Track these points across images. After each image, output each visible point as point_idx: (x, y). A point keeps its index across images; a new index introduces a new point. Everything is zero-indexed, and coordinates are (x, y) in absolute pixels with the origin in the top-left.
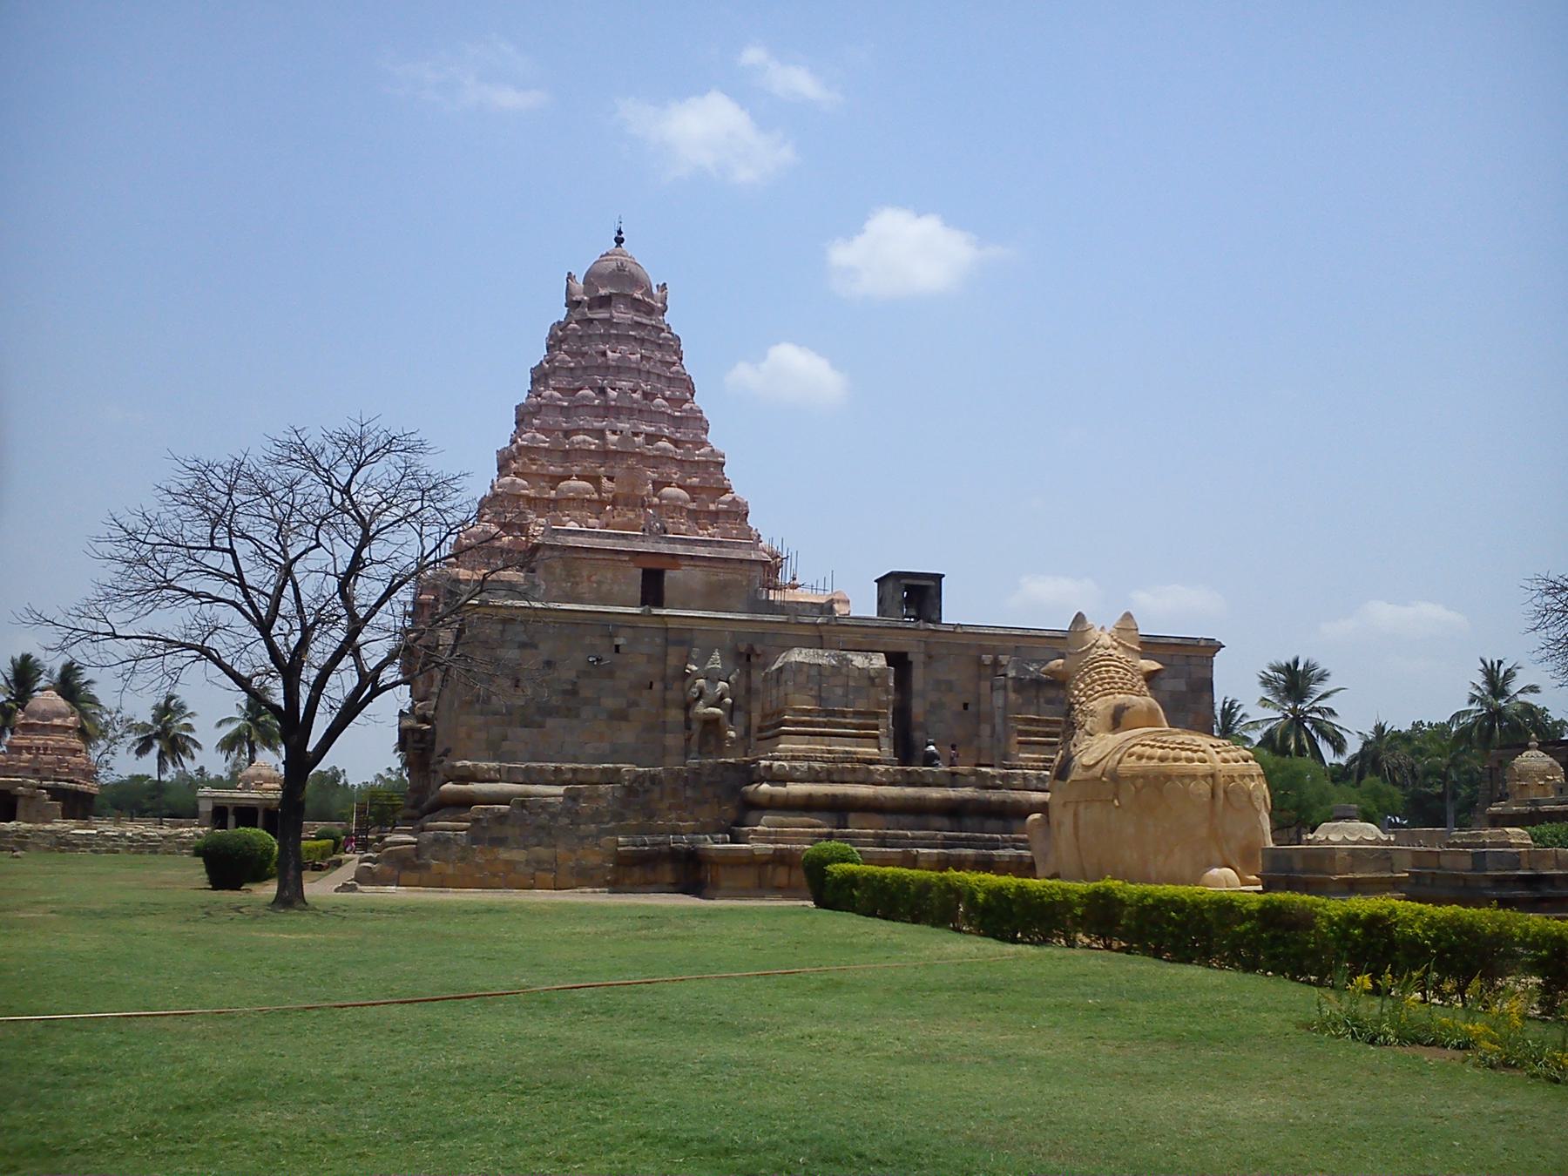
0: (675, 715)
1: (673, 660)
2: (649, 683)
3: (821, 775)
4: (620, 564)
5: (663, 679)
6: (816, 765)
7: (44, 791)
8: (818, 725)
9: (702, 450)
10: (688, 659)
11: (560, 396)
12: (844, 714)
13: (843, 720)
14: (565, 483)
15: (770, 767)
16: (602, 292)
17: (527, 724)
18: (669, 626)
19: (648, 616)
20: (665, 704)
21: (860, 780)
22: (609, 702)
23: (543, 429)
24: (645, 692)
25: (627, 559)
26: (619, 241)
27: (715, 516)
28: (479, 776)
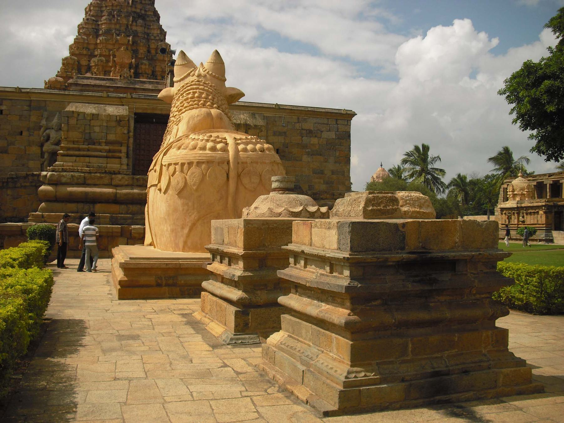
0: (35, 150)
1: (33, 118)
2: (20, 131)
3: (79, 180)
5: (28, 129)
6: (76, 174)
8: (83, 150)
12: (100, 144)
13: (98, 147)
15: (46, 175)
18: (32, 99)
19: (19, 93)
24: (18, 137)
25: (112, 90)
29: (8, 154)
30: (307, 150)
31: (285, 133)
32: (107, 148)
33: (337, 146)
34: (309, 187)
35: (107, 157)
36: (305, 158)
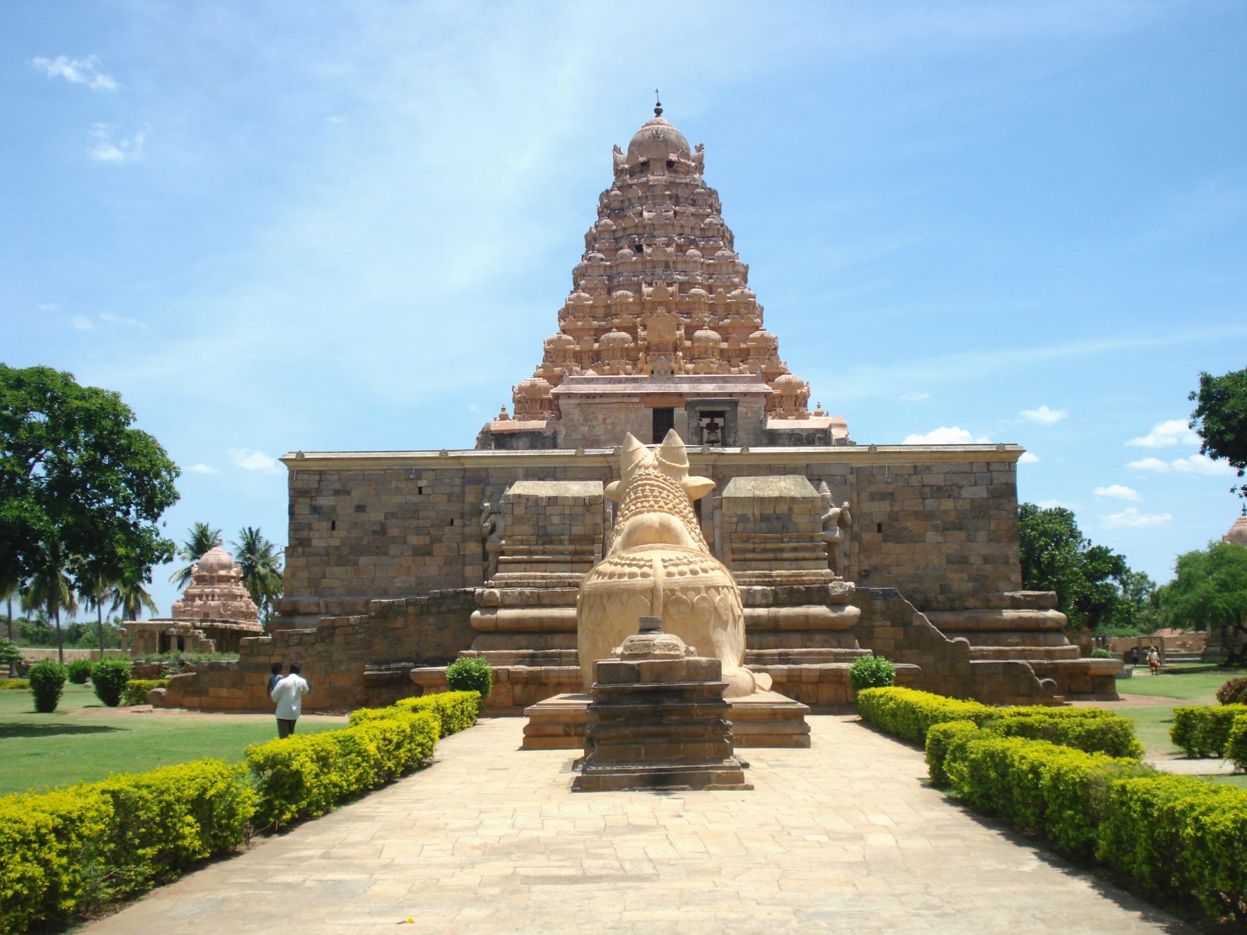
0: (473, 548)
1: (470, 499)
4: (631, 406)
5: (462, 516)
6: (527, 590)
7: (201, 631)
9: (733, 293)
10: (482, 496)
11: (603, 257)
12: (561, 543)
13: (559, 548)
14: (607, 334)
15: (482, 594)
16: (641, 159)
17: (341, 562)
18: (466, 467)
20: (465, 539)
21: (570, 603)
22: (414, 540)
23: (589, 289)
24: (447, 529)
26: (658, 112)
27: (744, 355)
28: (302, 610)
29: (433, 556)
30: (934, 522)
31: (892, 494)
32: (572, 548)
33: (992, 512)
34: (941, 588)
35: (572, 562)
36: (932, 537)
